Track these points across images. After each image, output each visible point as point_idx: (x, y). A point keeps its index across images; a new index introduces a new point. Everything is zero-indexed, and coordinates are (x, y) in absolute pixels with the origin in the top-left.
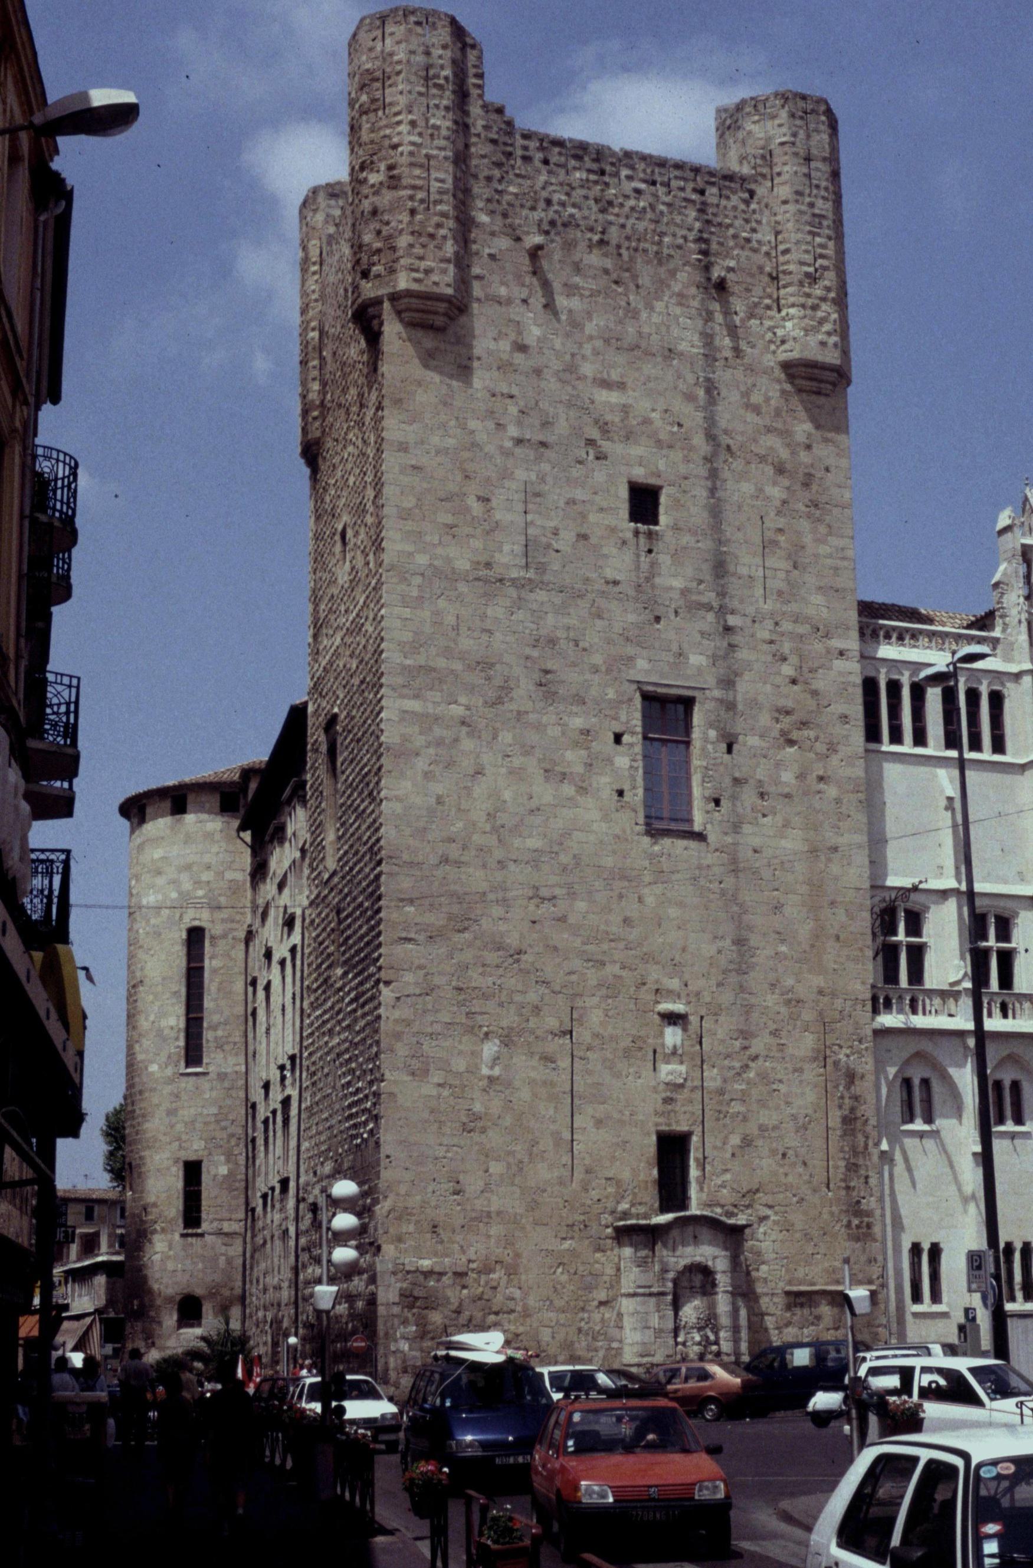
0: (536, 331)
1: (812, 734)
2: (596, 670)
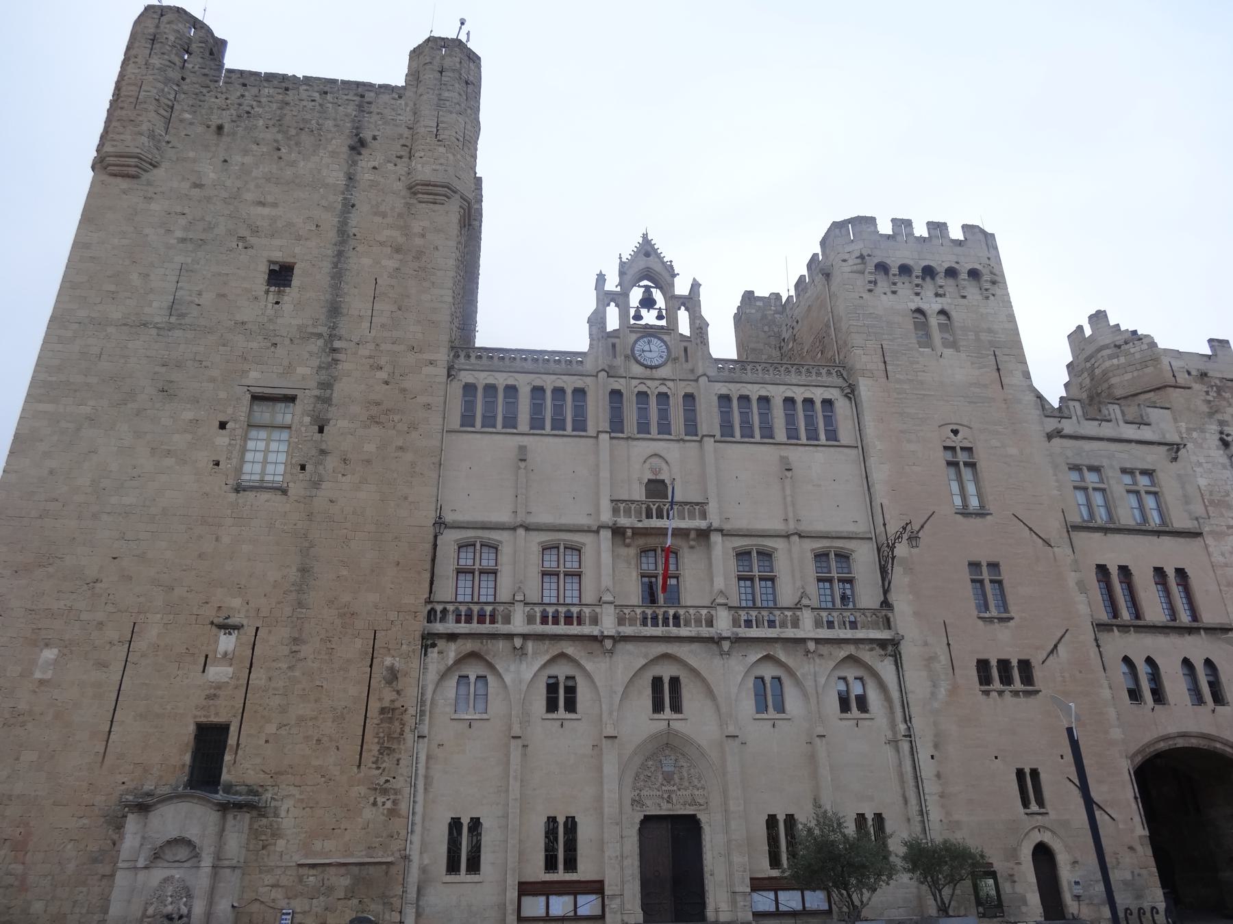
0: (212, 175)
1: (396, 418)
2: (212, 380)
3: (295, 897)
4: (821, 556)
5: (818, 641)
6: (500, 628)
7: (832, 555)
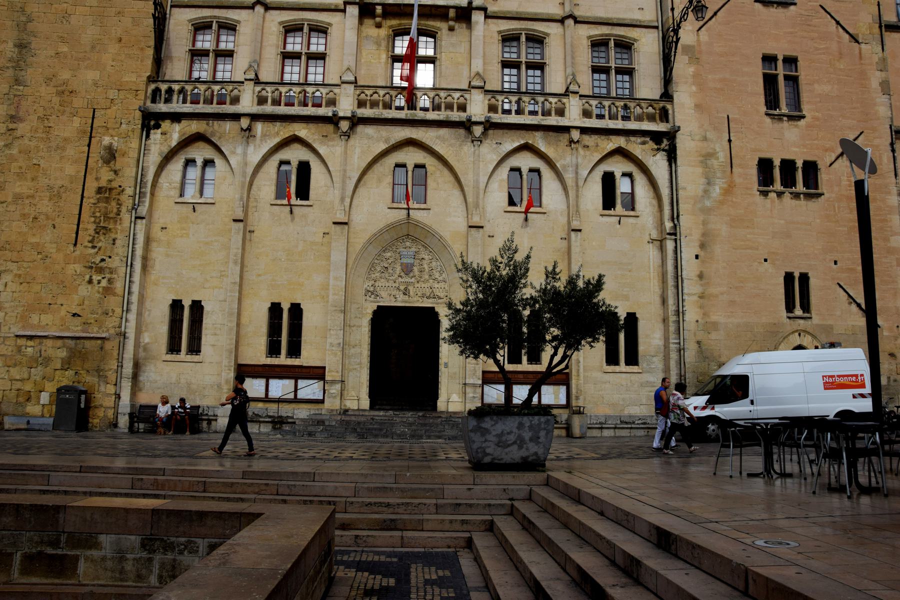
3: (15, 365)
4: (598, 44)
5: (584, 131)
6: (228, 109)
7: (612, 44)
